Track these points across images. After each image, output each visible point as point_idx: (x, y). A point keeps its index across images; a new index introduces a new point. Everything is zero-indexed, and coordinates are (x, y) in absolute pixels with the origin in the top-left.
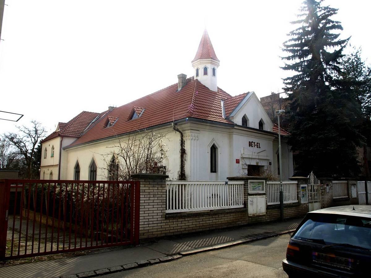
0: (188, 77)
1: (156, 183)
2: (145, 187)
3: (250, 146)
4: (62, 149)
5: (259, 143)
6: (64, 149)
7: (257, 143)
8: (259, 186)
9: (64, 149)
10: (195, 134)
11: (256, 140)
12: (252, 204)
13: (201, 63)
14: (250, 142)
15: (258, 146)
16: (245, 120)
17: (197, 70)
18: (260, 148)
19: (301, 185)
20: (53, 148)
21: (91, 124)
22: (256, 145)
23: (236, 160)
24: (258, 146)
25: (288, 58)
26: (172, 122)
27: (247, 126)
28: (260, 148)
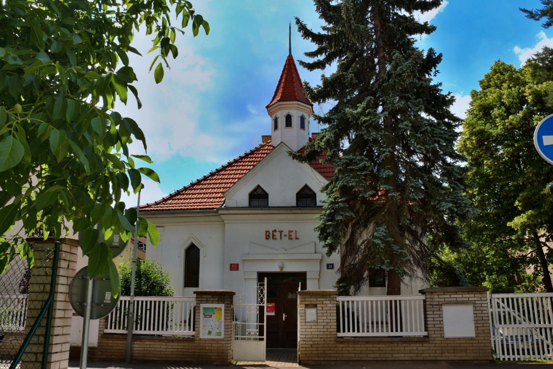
3: (266, 239)
5: (296, 231)
7: (290, 232)
11: (286, 228)
14: (267, 232)
18: (297, 239)
19: (201, 305)
22: (285, 236)
28: (297, 239)
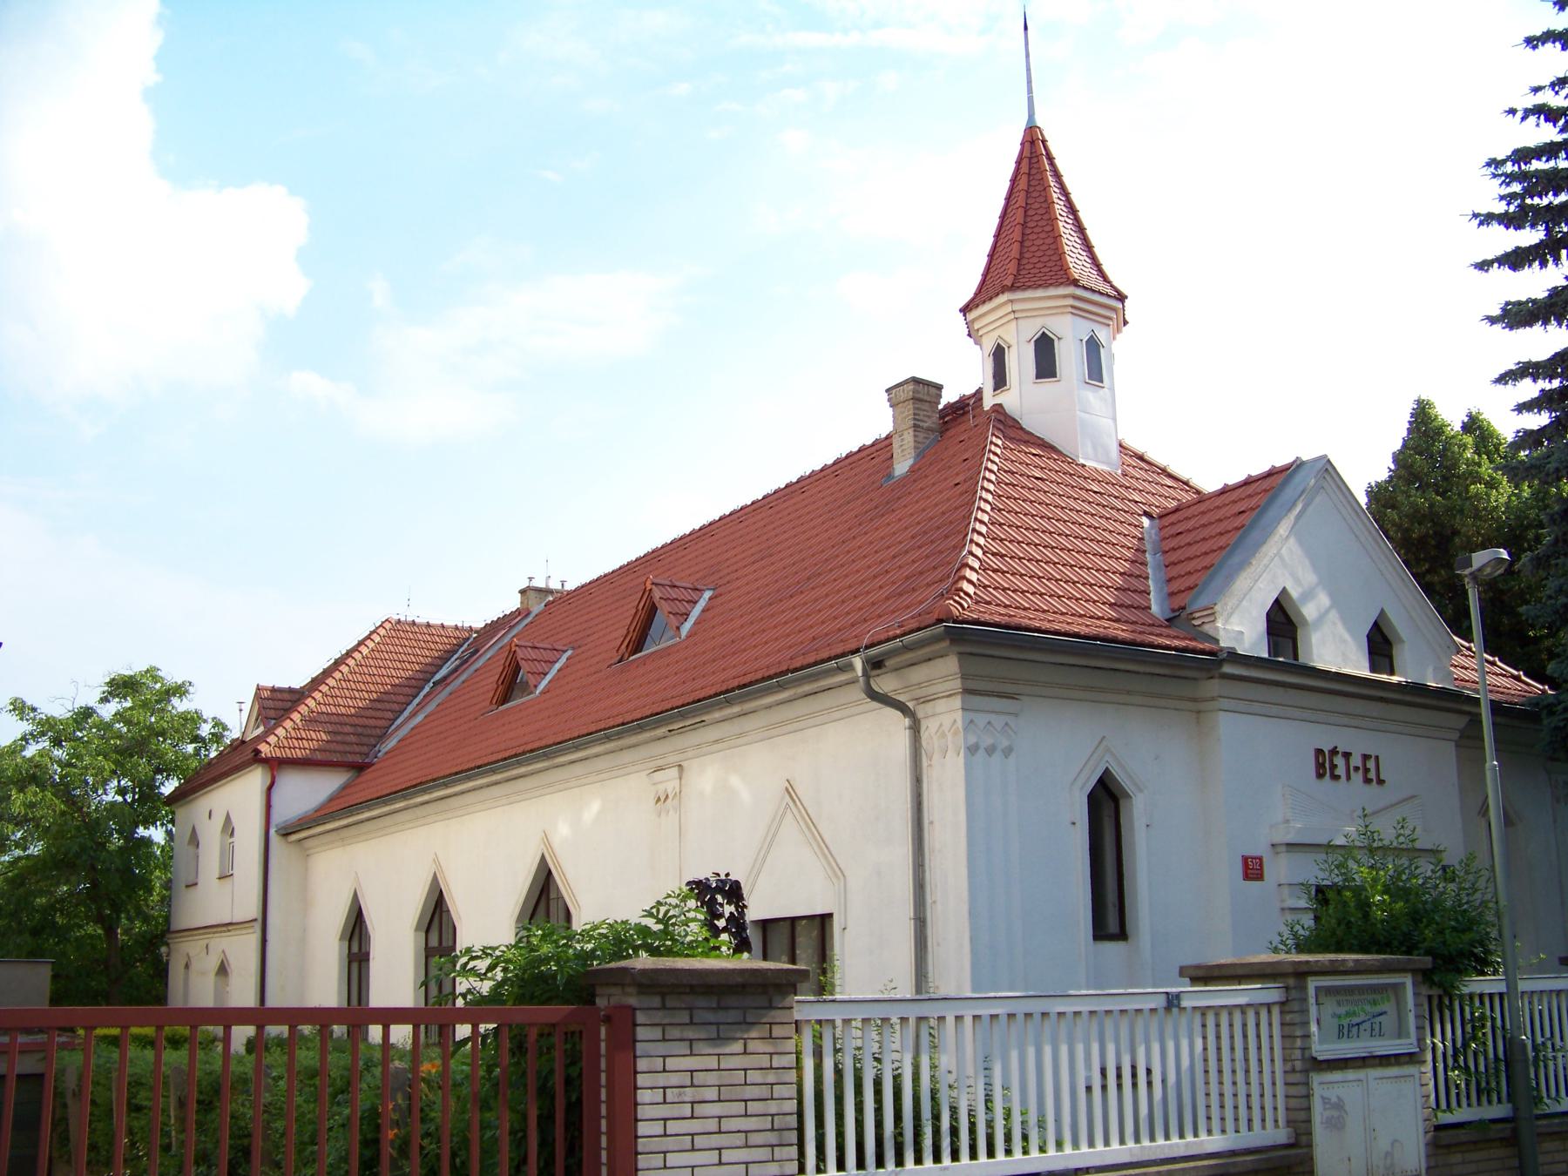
0: (949, 397)
1: (733, 1016)
2: (664, 1040)
3: (1320, 776)
4: (272, 831)
6: (286, 833)
7: (1366, 757)
8: (1378, 1009)
9: (286, 833)
10: (992, 718)
11: (1356, 742)
12: (1336, 1124)
13: (1016, 316)
14: (1319, 752)
15: (1372, 775)
16: (1282, 622)
17: (999, 355)
18: (1381, 782)
20: (228, 829)
21: (427, 689)
22: (1356, 769)
23: (1245, 859)
24: (1370, 771)
25: (1516, 259)
26: (856, 651)
27: (1296, 657)
28: (1381, 782)
